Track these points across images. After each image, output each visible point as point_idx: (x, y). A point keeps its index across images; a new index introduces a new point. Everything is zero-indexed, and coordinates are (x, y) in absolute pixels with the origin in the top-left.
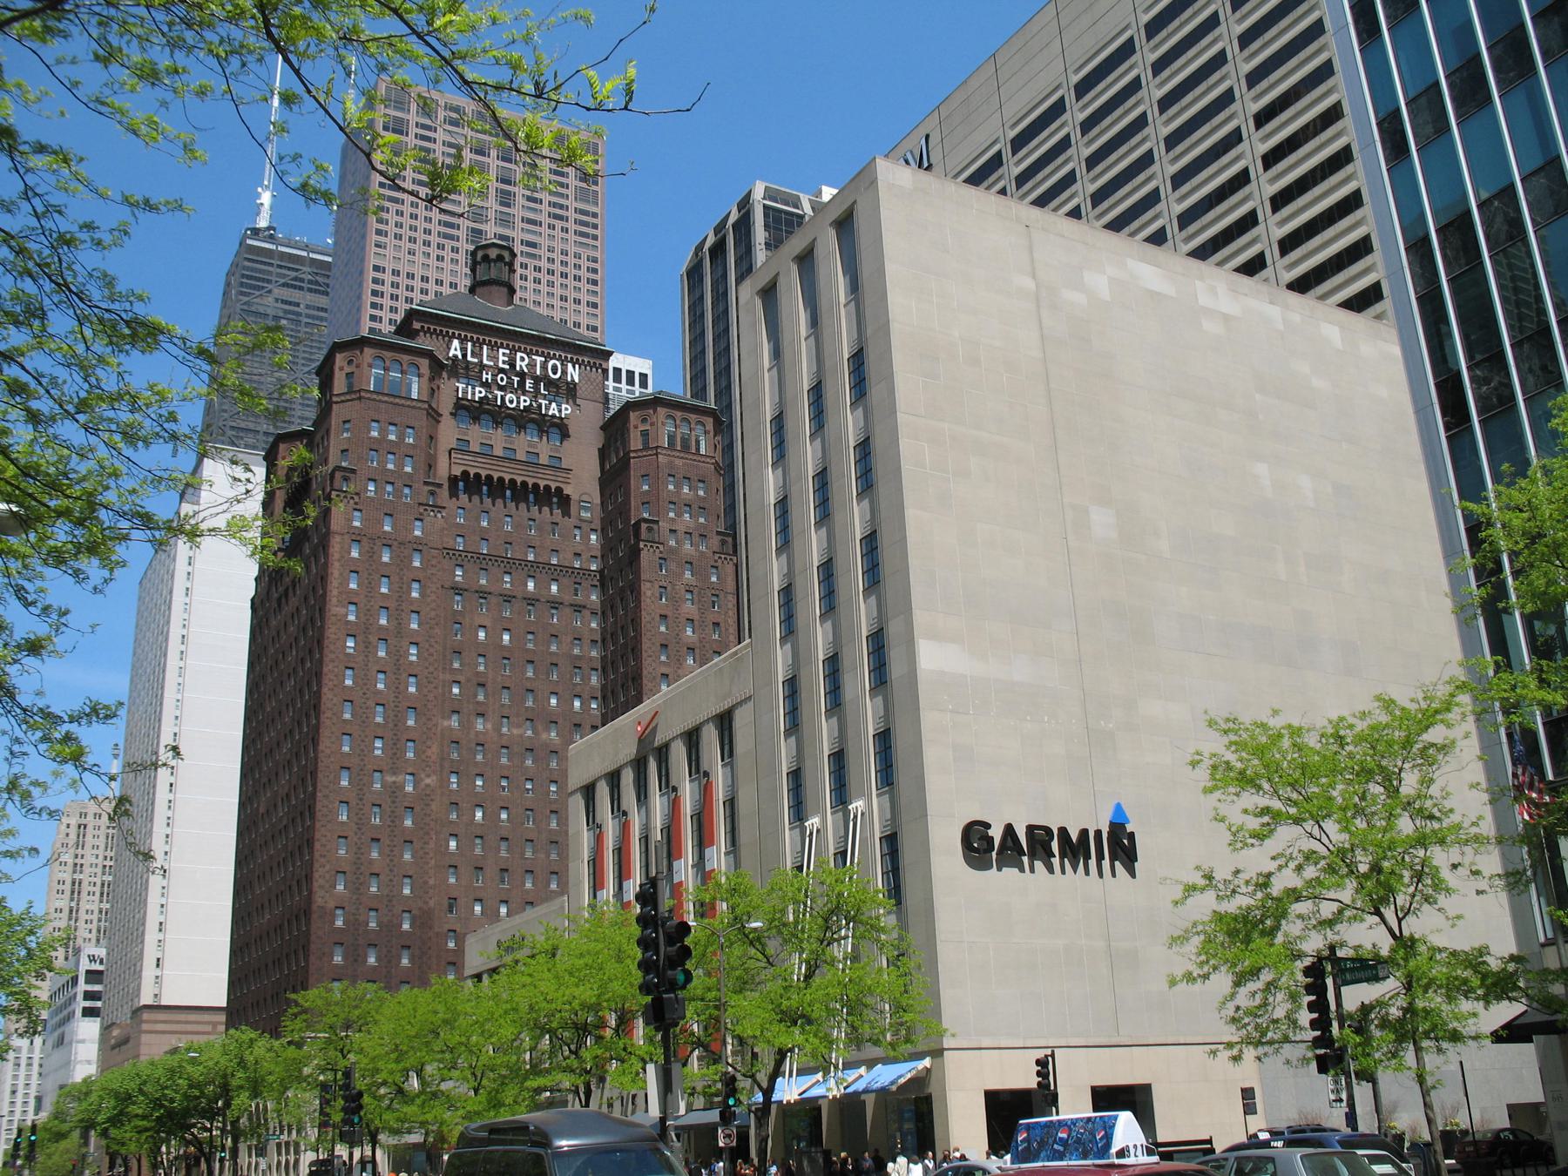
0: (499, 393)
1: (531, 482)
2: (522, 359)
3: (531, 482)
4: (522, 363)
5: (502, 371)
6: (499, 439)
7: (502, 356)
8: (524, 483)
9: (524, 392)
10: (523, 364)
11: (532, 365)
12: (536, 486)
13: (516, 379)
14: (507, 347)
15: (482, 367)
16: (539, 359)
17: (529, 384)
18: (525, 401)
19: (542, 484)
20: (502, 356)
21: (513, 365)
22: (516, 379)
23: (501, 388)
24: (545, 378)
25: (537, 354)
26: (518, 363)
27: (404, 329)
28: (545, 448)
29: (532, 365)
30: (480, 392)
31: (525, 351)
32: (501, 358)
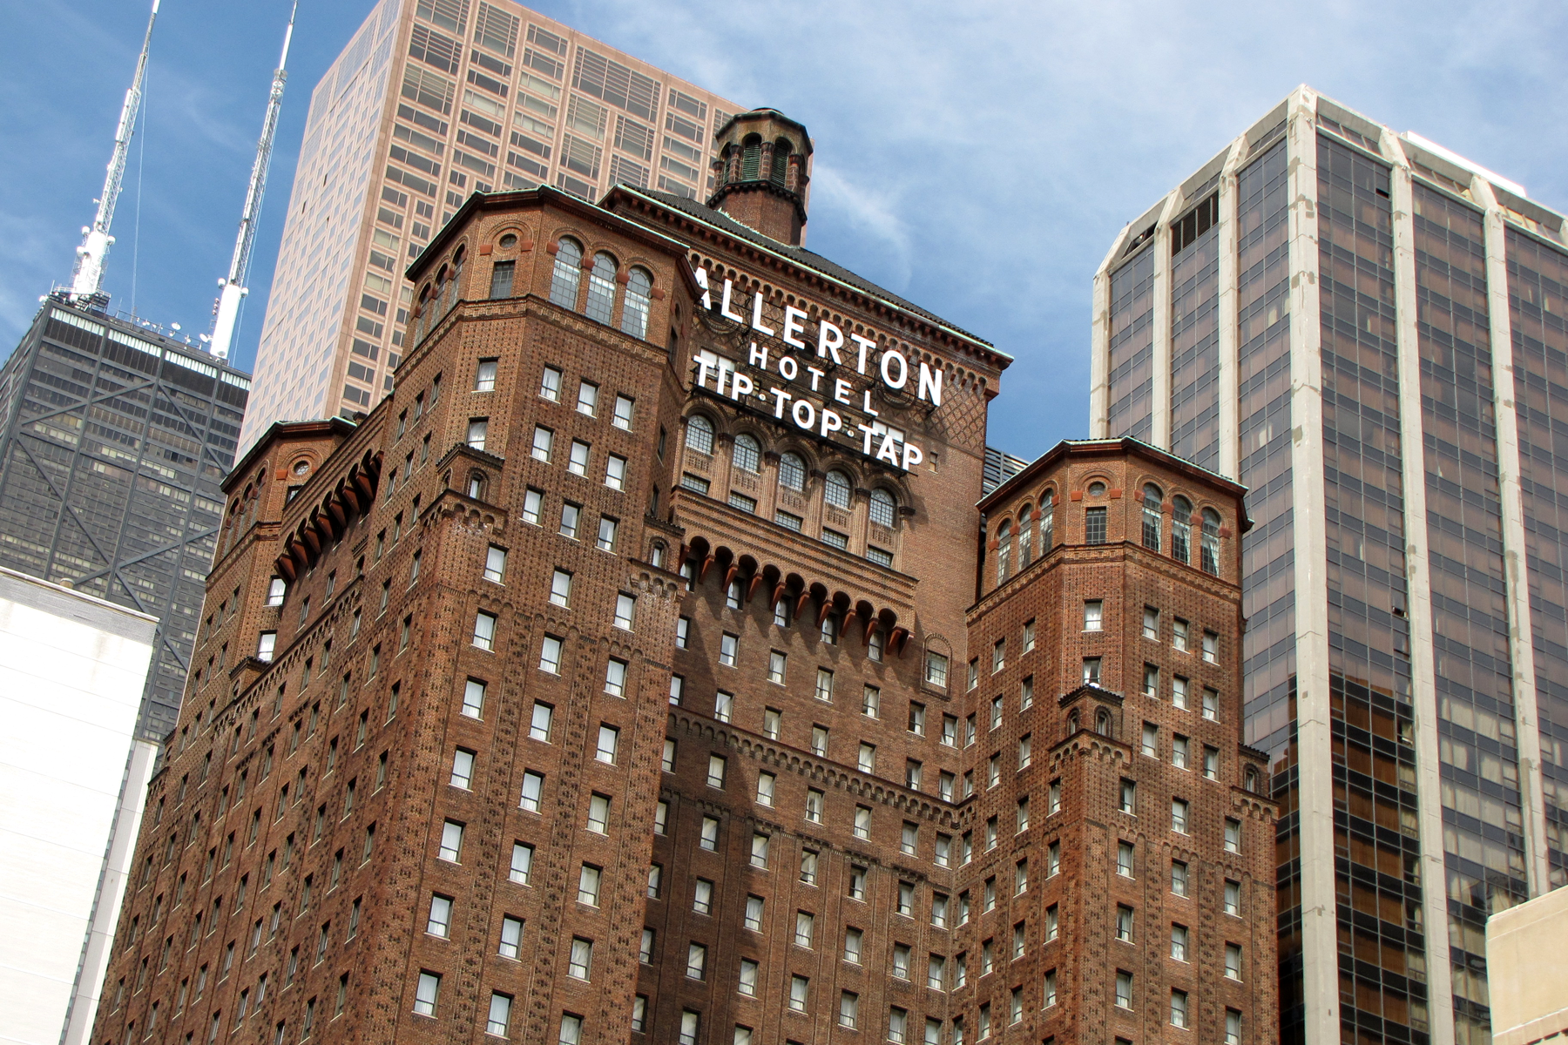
0: (782, 396)
1: (832, 588)
2: (832, 336)
3: (832, 588)
4: (829, 344)
5: (790, 351)
6: (771, 486)
7: (792, 321)
8: (819, 591)
9: (830, 402)
10: (834, 346)
11: (849, 352)
12: (842, 599)
13: (817, 373)
14: (802, 306)
15: (748, 333)
16: (865, 344)
17: (841, 388)
18: (831, 423)
19: (855, 597)
20: (792, 321)
21: (811, 340)
22: (817, 373)
23: (786, 385)
24: (873, 382)
25: (859, 330)
26: (823, 342)
27: (616, 199)
28: (864, 521)
29: (849, 352)
30: (742, 387)
31: (836, 320)
32: (790, 325)
